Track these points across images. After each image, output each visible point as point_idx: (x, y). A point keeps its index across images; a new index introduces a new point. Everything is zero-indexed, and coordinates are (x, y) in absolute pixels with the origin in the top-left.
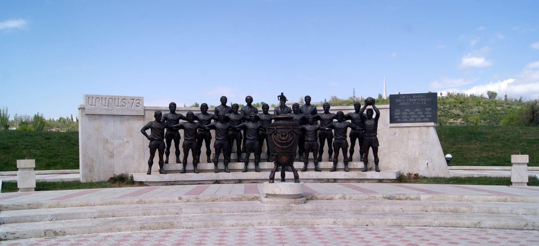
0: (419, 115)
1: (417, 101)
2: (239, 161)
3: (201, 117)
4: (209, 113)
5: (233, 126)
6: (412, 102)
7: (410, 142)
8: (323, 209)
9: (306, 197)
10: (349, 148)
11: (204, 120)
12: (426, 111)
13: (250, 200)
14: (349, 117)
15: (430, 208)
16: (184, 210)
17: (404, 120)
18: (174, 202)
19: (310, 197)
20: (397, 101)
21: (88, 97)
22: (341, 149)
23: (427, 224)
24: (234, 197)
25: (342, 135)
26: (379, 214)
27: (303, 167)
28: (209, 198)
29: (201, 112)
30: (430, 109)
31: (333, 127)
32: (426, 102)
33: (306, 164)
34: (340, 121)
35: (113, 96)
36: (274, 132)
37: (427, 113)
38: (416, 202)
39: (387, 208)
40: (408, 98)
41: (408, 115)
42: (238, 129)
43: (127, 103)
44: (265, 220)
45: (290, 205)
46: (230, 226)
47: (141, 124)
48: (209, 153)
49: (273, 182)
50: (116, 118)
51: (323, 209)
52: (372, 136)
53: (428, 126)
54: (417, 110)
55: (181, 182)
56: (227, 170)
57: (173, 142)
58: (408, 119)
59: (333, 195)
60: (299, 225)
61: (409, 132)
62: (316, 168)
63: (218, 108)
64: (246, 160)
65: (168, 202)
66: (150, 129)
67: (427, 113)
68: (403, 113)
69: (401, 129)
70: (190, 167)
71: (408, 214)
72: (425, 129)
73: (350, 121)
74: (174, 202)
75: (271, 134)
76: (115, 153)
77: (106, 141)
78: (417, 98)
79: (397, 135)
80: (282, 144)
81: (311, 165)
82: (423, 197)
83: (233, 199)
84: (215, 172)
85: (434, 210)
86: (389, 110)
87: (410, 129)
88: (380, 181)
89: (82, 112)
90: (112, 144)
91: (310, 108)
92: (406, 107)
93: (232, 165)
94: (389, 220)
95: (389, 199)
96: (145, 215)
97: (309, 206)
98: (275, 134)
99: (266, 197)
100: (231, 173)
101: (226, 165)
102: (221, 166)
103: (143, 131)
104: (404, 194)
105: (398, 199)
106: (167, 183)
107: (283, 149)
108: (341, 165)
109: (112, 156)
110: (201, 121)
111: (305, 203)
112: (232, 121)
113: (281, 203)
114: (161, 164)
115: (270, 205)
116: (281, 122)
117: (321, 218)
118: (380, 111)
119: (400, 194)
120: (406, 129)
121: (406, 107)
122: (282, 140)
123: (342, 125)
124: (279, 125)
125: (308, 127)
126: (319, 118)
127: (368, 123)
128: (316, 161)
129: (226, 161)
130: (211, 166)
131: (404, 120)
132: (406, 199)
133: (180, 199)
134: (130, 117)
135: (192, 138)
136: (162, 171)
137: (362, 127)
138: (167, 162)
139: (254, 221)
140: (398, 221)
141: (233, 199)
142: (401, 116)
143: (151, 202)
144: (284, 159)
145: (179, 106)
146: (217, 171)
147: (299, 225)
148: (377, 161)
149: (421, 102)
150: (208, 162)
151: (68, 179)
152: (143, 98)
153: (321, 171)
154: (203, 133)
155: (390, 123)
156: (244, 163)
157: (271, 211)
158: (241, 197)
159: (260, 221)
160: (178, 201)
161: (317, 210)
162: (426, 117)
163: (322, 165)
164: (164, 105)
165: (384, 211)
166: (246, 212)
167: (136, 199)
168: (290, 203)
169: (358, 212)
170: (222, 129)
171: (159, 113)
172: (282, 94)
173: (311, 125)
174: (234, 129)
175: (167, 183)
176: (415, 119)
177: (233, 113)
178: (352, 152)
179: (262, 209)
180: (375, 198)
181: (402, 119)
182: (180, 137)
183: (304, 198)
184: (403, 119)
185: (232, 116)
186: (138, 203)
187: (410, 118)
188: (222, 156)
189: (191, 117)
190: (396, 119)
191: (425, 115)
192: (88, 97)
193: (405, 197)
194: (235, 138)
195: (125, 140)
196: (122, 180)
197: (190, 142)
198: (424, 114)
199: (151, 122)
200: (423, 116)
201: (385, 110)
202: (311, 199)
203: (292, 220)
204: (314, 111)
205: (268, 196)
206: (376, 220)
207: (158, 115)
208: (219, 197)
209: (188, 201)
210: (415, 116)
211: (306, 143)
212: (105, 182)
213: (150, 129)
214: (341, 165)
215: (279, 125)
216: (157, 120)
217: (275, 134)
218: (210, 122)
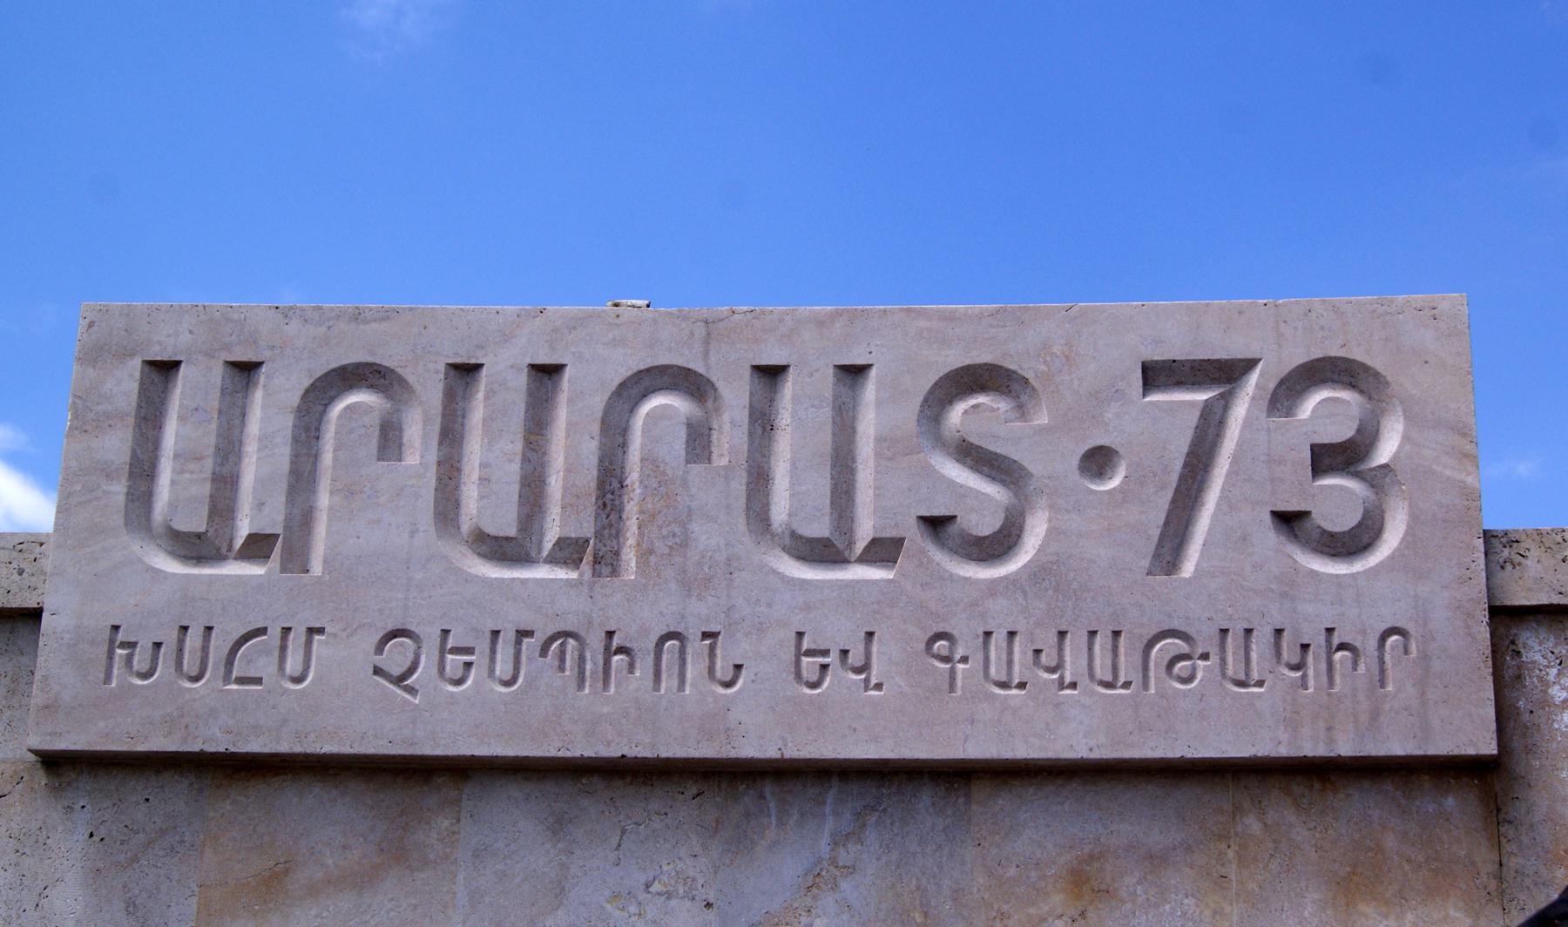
43: (1050, 459)
134: (1133, 824)
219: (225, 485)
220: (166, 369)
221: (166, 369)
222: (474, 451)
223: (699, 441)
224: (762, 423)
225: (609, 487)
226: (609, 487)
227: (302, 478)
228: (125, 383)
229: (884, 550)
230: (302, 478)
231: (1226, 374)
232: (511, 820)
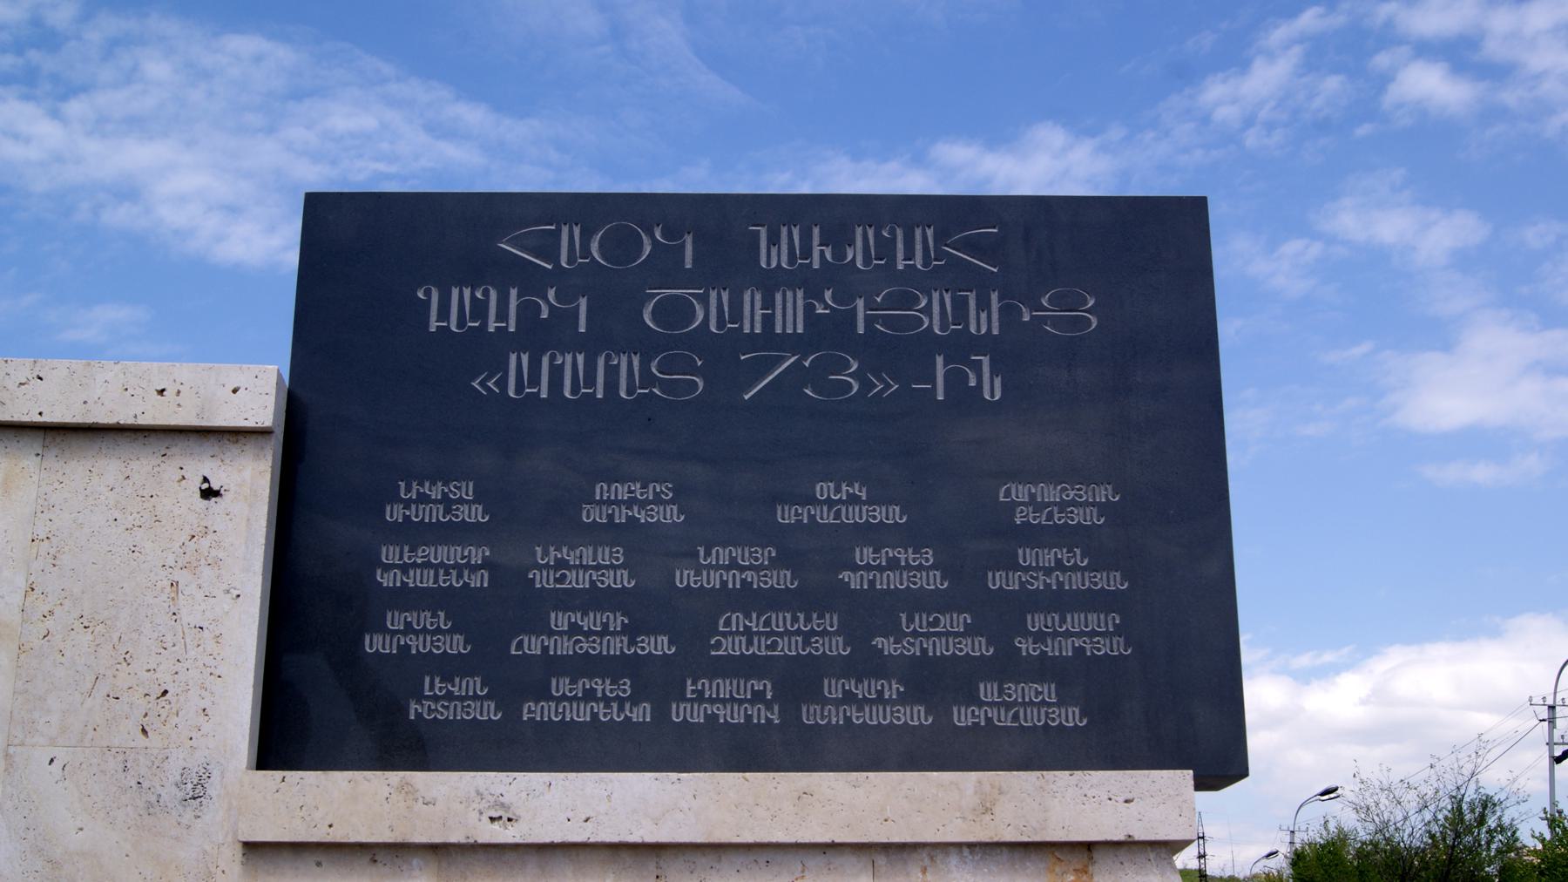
0: (870, 614)
1: (827, 334)
6: (726, 354)
12: (1010, 537)
17: (564, 705)
20: (447, 309)
30: (1086, 503)
37: (1038, 568)
40: (665, 267)
41: (643, 608)
54: (837, 501)
58: (654, 681)
67: (1038, 568)
78: (837, 276)
86: (251, 481)
131: (564, 705)
142: (496, 616)
149: (900, 351)
162: (1006, 667)
176: (798, 681)
181: (517, 682)
184: (535, 679)
187: (696, 660)
190: (412, 669)
191: (1002, 617)
198: (966, 590)
200: (953, 638)
201: (172, 478)
210: (782, 637)
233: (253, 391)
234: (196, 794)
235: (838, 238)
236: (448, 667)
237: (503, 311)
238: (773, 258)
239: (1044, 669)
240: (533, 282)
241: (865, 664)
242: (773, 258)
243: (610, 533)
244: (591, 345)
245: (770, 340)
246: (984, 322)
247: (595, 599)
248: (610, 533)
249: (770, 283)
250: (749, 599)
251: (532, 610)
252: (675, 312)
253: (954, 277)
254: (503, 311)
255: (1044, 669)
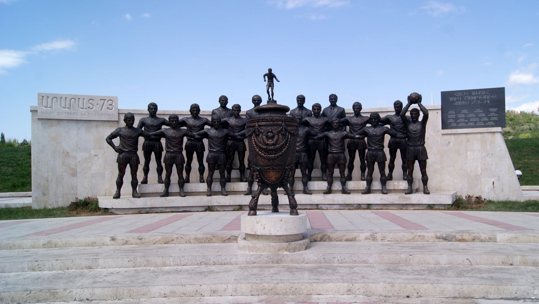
1: (477, 99)
2: (241, 181)
3: (191, 122)
4: (202, 117)
5: (232, 133)
6: (470, 101)
7: (469, 153)
8: (336, 260)
9: (308, 239)
10: (387, 163)
11: (194, 126)
12: (490, 112)
13: (224, 242)
14: (387, 121)
15: (517, 259)
16: (101, 262)
17: (461, 125)
18: (103, 244)
19: (320, 236)
20: (451, 99)
21: (42, 97)
22: (376, 163)
23: (519, 295)
24: (200, 236)
25: (377, 144)
26: (430, 271)
27: (325, 188)
28: (159, 238)
29: (191, 116)
30: (495, 110)
31: (365, 134)
32: (490, 100)
33: (330, 184)
34: (374, 126)
35: (76, 96)
36: (254, 132)
37: (492, 114)
38: (490, 244)
39: (444, 259)
40: (466, 95)
41: (466, 118)
42: (239, 137)
43: (95, 104)
44: (224, 286)
45: (280, 253)
46: (160, 296)
47: (109, 131)
48: (201, 170)
49: (255, 214)
50: (81, 124)
51: (336, 260)
52: (420, 145)
53: (494, 132)
54: (478, 111)
55: (160, 209)
56: (224, 193)
57: (153, 155)
58: (466, 123)
59: (356, 234)
60: (286, 294)
61: (468, 141)
62: (343, 189)
63: (216, 111)
64: (250, 178)
65: (93, 244)
66: (118, 137)
67: (492, 114)
68: (459, 116)
69: (456, 136)
70: (174, 188)
71: (480, 271)
72: (489, 136)
73: (388, 126)
74: (103, 244)
75: (250, 136)
76: (79, 169)
77: (67, 154)
78: (478, 95)
79: (451, 144)
80: (267, 151)
81: (337, 185)
82: (502, 236)
83: (198, 240)
84: (208, 195)
85: (525, 263)
86: (440, 112)
87: (469, 136)
88: (430, 207)
89: (33, 116)
90: (75, 158)
91: (336, 110)
92: (463, 107)
93: (231, 186)
94: (450, 286)
95: (445, 239)
96: (34, 270)
97: (311, 255)
98: (257, 135)
99: (245, 239)
100: (229, 197)
101: (223, 185)
102: (216, 186)
103: (110, 140)
104: (468, 232)
105: (460, 240)
106: (140, 211)
107: (269, 159)
108: (377, 185)
109: (74, 174)
110: (190, 128)
111: (306, 248)
112: (232, 127)
113: (266, 249)
114: (134, 184)
115: (247, 253)
116: (266, 115)
117: (325, 281)
118: (430, 114)
119: (462, 232)
120: (464, 136)
121: (463, 107)
122: (267, 145)
123: (378, 131)
124: (263, 120)
125: (332, 134)
126: (347, 123)
127: (413, 127)
128: (344, 180)
129: (223, 180)
130: (203, 187)
131: (461, 125)
132: (474, 240)
133: (113, 239)
134: (99, 123)
135: (175, 149)
136: (135, 195)
137: (404, 133)
138: (145, 182)
139: (204, 287)
140: (466, 290)
141: (198, 240)
143: (66, 245)
144: (273, 176)
145: (161, 109)
146: (210, 193)
147: (286, 294)
148: (425, 180)
149: (482, 100)
150: (201, 182)
151: (15, 204)
152: (117, 98)
153: (349, 193)
154: (194, 143)
155: (442, 129)
156: (247, 183)
157: (248, 263)
158: (210, 236)
159: (214, 287)
160: (110, 243)
161: (325, 262)
162: (490, 121)
163: (351, 185)
164: (139, 107)
165: (438, 263)
166: (206, 264)
167: (43, 240)
168: (279, 250)
169: (393, 268)
170: (217, 138)
171: (130, 116)
172: (270, 70)
173: (335, 131)
174: (234, 138)
175: (140, 211)
176: (476, 122)
177: (233, 117)
178: (392, 167)
179: (233, 260)
180: (422, 238)
182: (160, 148)
183: (306, 241)
184: (459, 123)
185: (232, 121)
186: (44, 245)
187: (469, 121)
188: (217, 174)
189: (175, 121)
190: (450, 123)
192: (42, 97)
193: (471, 237)
194: (236, 150)
195: (93, 152)
196: (86, 206)
197: (173, 155)
198: (487, 116)
199: (120, 128)
202: (322, 240)
203: (272, 285)
204: (342, 113)
205: (247, 236)
206: (425, 286)
207: (129, 119)
208: (175, 236)
209: (126, 243)
210: (475, 120)
211: (330, 155)
212: (62, 209)
213: (118, 137)
214: (377, 185)
215: (263, 120)
216: (127, 125)
217: (257, 135)
218: (202, 128)
219: (47, 104)
220: (43, 97)
221: (43, 97)
222: (62, 102)
223: (75, 102)
224: (79, 101)
225: (70, 104)
226: (70, 104)
227: (52, 103)
228: (41, 98)
229: (86, 109)
230: (52, 103)
231: (105, 100)
232: (65, 122)
233: (440, 108)
234: (439, 131)
235: (478, 92)
236: (453, 123)
237: (455, 99)
238: (473, 94)
239: (492, 121)
240: (457, 97)
241: (480, 121)
242: (473, 94)
243: (463, 114)
244: (461, 101)
245: (473, 100)
246: (488, 98)
247: (462, 118)
248: (463, 114)
249: (473, 96)
250: (472, 117)
251: (458, 119)
252: (467, 98)
253: (486, 94)
254: (455, 99)
255: (492, 121)
